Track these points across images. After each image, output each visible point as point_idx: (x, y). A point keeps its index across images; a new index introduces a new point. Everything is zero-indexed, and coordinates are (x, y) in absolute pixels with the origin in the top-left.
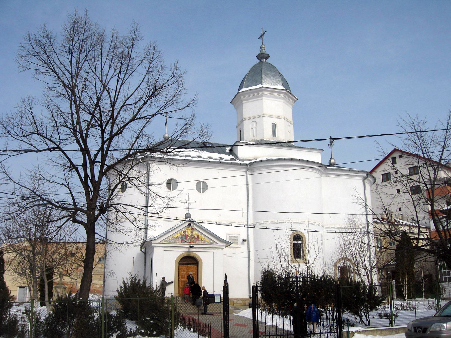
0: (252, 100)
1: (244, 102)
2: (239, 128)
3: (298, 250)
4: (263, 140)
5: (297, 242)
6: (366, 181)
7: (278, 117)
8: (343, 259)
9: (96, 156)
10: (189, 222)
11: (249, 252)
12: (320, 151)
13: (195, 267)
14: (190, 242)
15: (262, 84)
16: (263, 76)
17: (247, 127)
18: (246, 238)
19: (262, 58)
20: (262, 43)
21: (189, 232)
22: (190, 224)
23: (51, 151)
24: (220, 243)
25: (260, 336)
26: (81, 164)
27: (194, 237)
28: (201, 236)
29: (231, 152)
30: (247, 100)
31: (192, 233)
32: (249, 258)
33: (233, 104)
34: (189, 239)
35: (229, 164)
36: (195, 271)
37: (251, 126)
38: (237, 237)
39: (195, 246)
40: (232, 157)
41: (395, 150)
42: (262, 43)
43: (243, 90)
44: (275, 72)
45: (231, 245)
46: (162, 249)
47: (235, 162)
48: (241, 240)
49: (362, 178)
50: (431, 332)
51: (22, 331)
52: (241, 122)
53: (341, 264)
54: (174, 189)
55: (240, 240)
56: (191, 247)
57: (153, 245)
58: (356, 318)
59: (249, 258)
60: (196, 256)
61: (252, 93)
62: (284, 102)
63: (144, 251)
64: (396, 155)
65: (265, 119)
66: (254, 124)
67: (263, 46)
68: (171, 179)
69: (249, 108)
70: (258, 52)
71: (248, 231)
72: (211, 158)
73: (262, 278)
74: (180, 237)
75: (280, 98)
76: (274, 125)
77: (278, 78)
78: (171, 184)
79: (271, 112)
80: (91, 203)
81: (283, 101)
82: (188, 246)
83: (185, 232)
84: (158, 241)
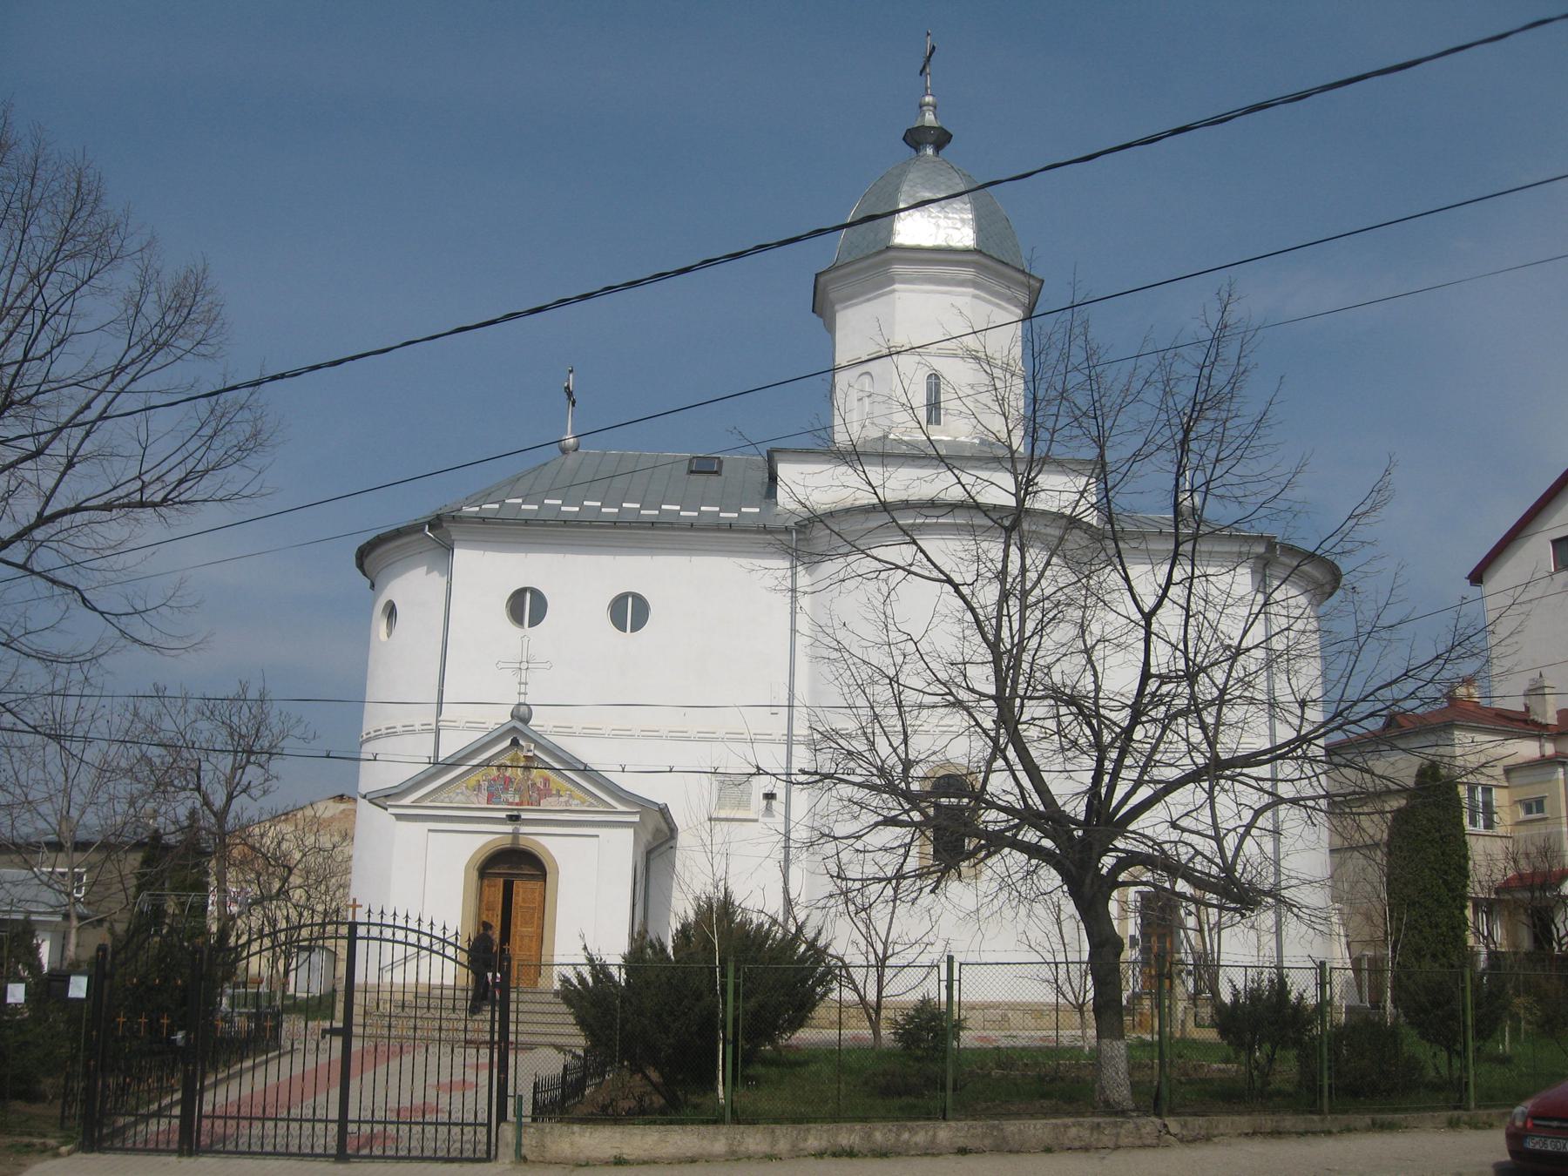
1: (837, 307)
22: (515, 743)
24: (621, 808)
25: (207, 1117)
27: (534, 784)
33: (820, 316)
34: (517, 791)
39: (524, 816)
54: (532, 624)
62: (975, 296)
66: (866, 379)
74: (485, 785)
75: (962, 283)
77: (961, 210)
78: (526, 606)
81: (971, 290)
82: (503, 815)
84: (407, 801)
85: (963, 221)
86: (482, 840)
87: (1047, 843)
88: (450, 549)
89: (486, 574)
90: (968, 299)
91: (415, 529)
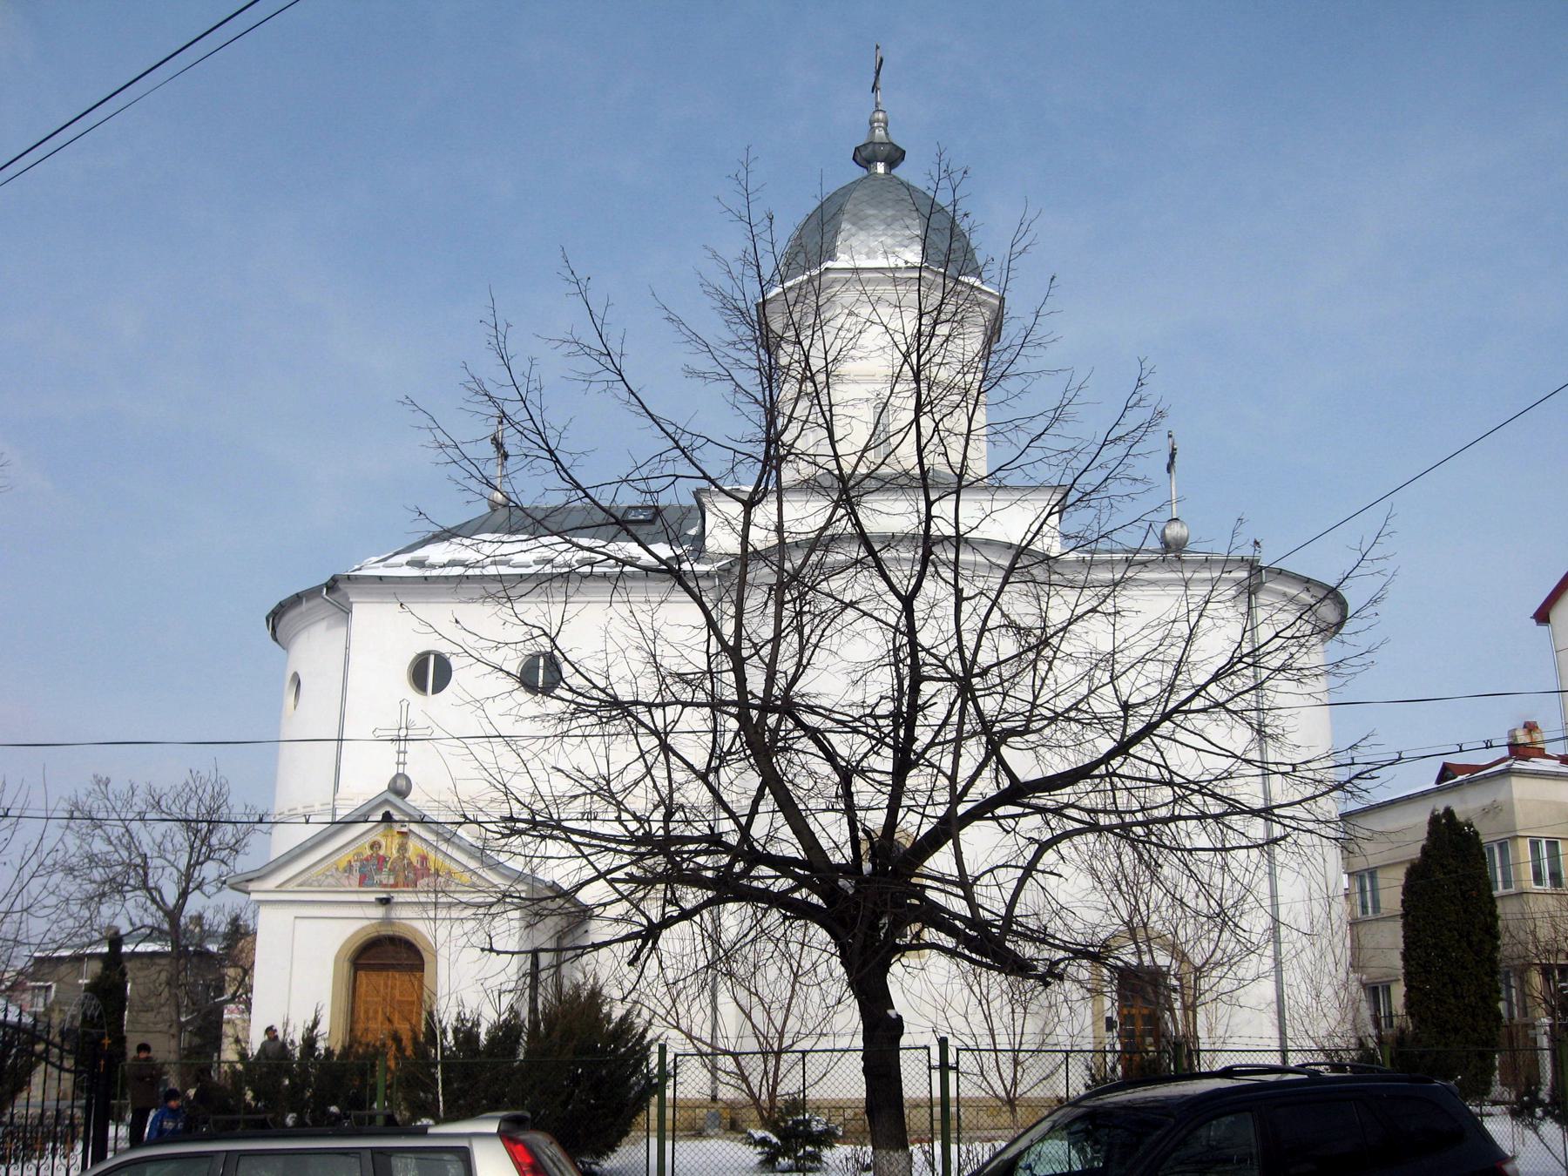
14: (392, 881)
16: (845, 226)
20: (877, 104)
21: (390, 848)
27: (410, 863)
31: (403, 848)
39: (398, 898)
42: (877, 104)
46: (289, 913)
54: (437, 690)
60: (410, 937)
67: (880, 115)
68: (428, 653)
74: (356, 865)
82: (372, 898)
84: (271, 883)
86: (355, 926)
87: (815, 899)
88: (347, 611)
89: (384, 635)
91: (313, 593)
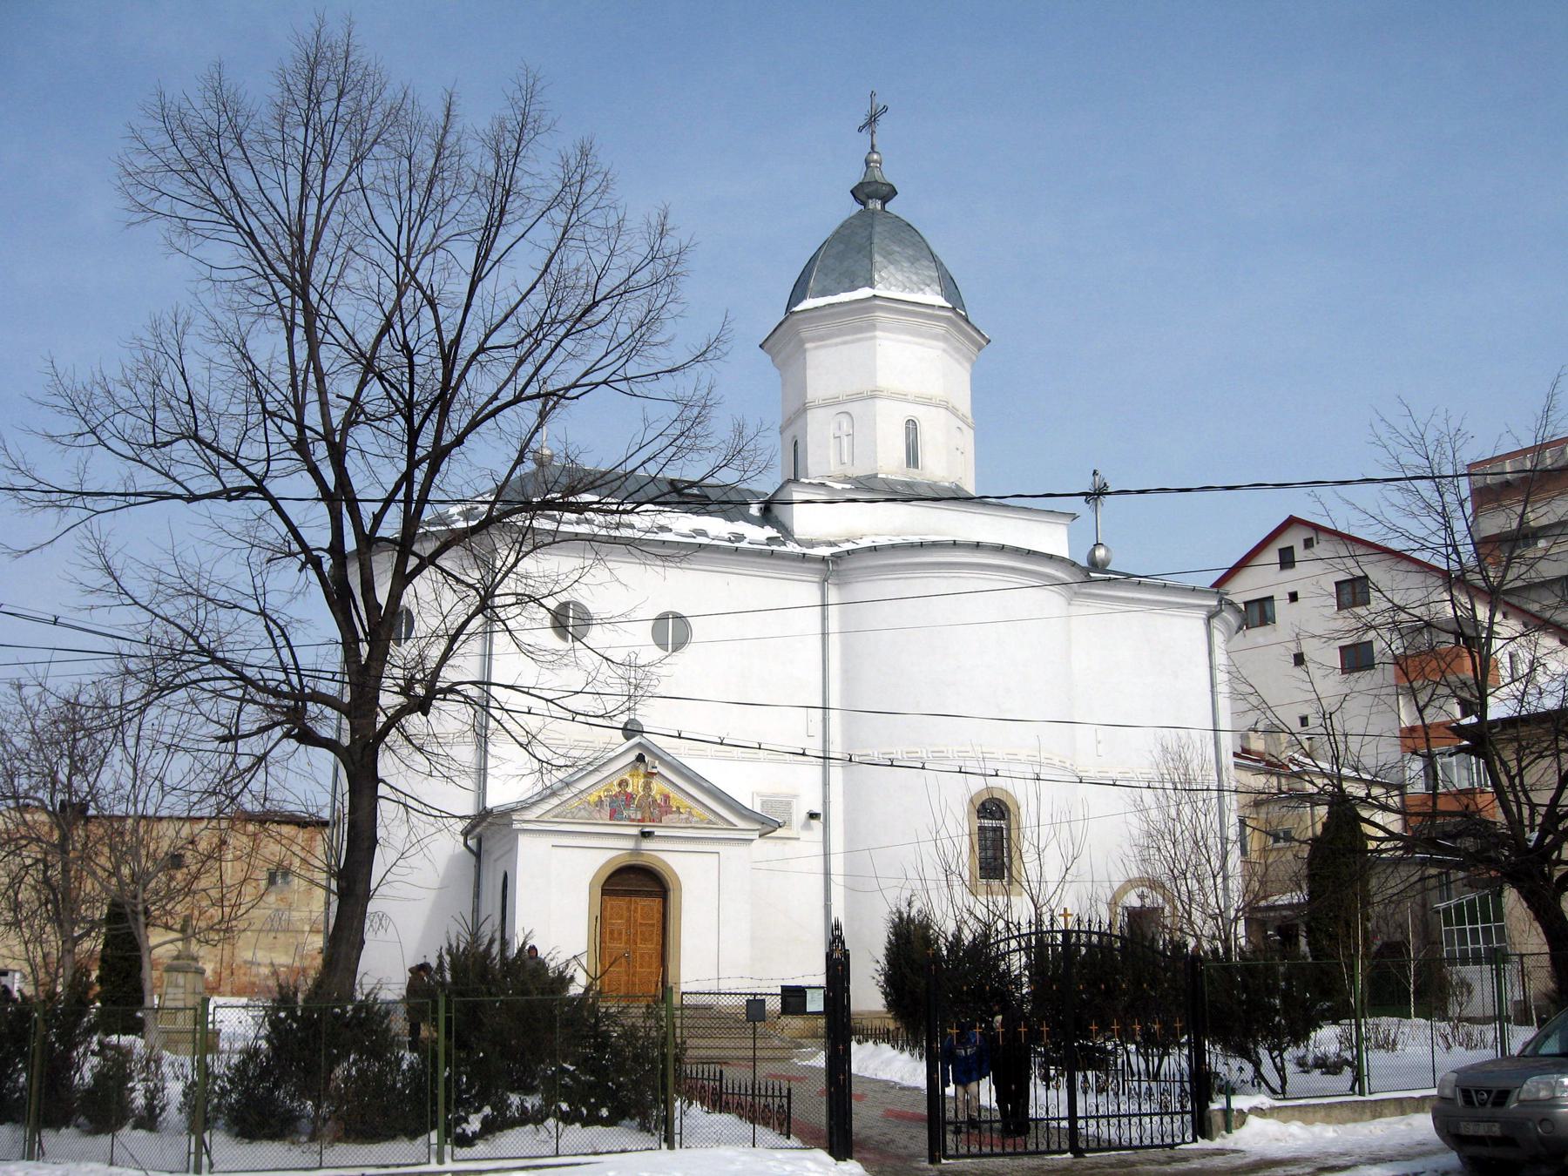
0: (838, 340)
2: (789, 434)
3: (995, 854)
4: (875, 476)
5: (987, 823)
6: (1215, 622)
7: (927, 402)
8: (1140, 882)
9: (377, 519)
10: (637, 752)
11: (827, 855)
12: (1067, 521)
13: (656, 903)
15: (872, 286)
16: (877, 258)
17: (820, 431)
18: (818, 809)
19: (870, 197)
21: (636, 785)
22: (640, 758)
23: (230, 499)
24: (741, 824)
26: (326, 545)
27: (655, 801)
28: (677, 798)
29: (768, 515)
30: (822, 338)
31: (647, 786)
32: (827, 874)
33: (768, 352)
34: (639, 807)
35: (765, 556)
36: (657, 916)
37: (832, 429)
38: (789, 804)
39: (658, 832)
40: (770, 532)
41: (1292, 522)
43: (808, 303)
44: (913, 244)
45: (779, 832)
47: (783, 548)
48: (803, 815)
49: (1203, 614)
50: (1522, 1103)
51: (150, 1107)
52: (798, 413)
53: (1133, 900)
55: (800, 815)
56: (646, 835)
57: (516, 826)
58: (1241, 1069)
59: (827, 874)
61: (832, 315)
63: (474, 848)
64: (1294, 539)
65: (879, 403)
66: (845, 421)
67: (875, 157)
69: (828, 366)
70: (856, 177)
71: (826, 783)
72: (703, 533)
73: (890, 942)
74: (607, 801)
75: (935, 337)
76: (912, 427)
77: (928, 268)
79: (897, 383)
80: (364, 678)
81: (941, 345)
82: (635, 831)
83: (623, 783)
85: (931, 278)
90: (940, 352)
